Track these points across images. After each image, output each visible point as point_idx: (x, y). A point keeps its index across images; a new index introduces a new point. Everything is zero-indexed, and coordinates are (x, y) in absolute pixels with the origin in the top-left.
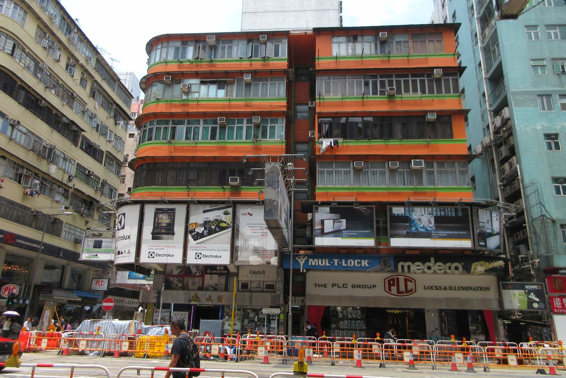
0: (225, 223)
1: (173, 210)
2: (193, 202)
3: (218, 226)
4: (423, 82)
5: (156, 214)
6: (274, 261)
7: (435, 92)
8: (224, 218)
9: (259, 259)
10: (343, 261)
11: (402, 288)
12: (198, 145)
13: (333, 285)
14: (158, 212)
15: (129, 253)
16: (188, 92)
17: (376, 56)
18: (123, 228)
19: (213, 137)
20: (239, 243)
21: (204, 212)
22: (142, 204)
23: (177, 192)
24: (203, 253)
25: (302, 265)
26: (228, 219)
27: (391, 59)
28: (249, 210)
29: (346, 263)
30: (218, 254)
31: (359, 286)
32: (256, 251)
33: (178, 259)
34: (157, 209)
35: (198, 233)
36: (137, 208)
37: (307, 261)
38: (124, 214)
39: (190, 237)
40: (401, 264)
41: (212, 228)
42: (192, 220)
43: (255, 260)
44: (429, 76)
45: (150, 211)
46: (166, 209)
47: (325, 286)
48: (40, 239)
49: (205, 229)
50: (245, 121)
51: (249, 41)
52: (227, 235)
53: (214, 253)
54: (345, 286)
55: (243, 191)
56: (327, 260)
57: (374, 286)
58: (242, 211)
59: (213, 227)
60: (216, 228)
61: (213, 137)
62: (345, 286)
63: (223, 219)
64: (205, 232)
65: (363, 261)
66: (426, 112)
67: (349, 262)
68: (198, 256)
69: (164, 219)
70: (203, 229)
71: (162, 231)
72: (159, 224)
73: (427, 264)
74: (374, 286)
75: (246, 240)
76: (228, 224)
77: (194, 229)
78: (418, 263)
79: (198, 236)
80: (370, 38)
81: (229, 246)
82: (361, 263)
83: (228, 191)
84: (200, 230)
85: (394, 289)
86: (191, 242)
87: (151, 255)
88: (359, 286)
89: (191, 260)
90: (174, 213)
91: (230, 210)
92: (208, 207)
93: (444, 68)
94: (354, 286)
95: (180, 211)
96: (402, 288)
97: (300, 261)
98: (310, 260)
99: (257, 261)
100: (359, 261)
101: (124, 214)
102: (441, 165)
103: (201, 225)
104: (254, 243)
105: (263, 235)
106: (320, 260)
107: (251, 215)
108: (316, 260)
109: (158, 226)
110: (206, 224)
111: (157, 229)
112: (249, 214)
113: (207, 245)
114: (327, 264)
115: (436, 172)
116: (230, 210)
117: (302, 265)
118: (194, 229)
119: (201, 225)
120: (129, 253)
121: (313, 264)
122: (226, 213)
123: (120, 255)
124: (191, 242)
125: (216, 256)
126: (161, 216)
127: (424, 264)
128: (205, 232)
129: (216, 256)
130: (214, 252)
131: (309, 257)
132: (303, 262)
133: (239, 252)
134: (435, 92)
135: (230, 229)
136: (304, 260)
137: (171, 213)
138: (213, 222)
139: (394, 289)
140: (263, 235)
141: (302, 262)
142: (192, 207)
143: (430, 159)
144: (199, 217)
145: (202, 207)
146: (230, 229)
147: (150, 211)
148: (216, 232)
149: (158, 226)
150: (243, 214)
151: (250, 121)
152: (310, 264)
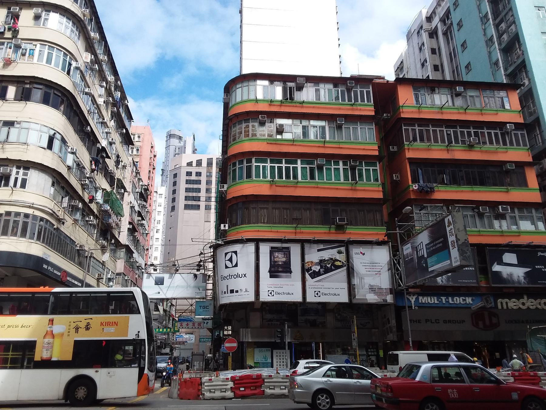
0: (340, 261)
1: (288, 248)
2: (309, 241)
3: (333, 265)
4: (496, 135)
5: (271, 253)
6: (390, 299)
7: (508, 144)
8: (338, 257)
9: (376, 297)
10: (450, 299)
11: (487, 322)
12: (299, 185)
13: (427, 321)
14: (273, 251)
15: (246, 291)
16: (280, 130)
17: (453, 107)
18: (236, 265)
19: (312, 177)
20: (356, 281)
21: (319, 250)
22: (257, 242)
23: (285, 231)
24: (275, 290)
25: (413, 302)
26: (342, 258)
27: (467, 111)
28: (361, 250)
29: (453, 300)
30: (337, 292)
31: (450, 321)
32: (372, 289)
33: (297, 298)
34: (272, 248)
35: (314, 271)
36: (251, 247)
37: (417, 299)
38: (236, 252)
39: (307, 276)
40: (499, 300)
41: (328, 267)
42: (307, 258)
43: (372, 298)
44: (501, 129)
45: (265, 249)
46: (280, 247)
47: (419, 321)
48: (81, 277)
49: (321, 267)
50: (341, 163)
51: (335, 86)
52: (342, 273)
53: (332, 291)
54: (437, 321)
55: (348, 231)
56: (436, 298)
57: (463, 321)
58: (355, 251)
59: (329, 266)
60: (331, 266)
61: (312, 177)
62: (437, 321)
63: (338, 258)
64: (322, 270)
65: (467, 298)
66: (505, 162)
67: (455, 299)
68: (317, 294)
69: (280, 258)
70: (319, 267)
71: (279, 270)
72: (275, 262)
73: (522, 301)
74: (463, 321)
75: (361, 279)
76: (343, 263)
77: (311, 267)
78: (514, 300)
79: (314, 275)
80: (446, 91)
81: (345, 285)
82: (465, 300)
83: (333, 230)
84: (317, 268)
85: (481, 324)
86: (310, 281)
87: (317, 294)
88: (450, 321)
89: (311, 298)
90: (290, 252)
91: (343, 249)
92: (322, 247)
93: (515, 124)
94: (445, 322)
95: (295, 250)
96: (487, 322)
97: (410, 299)
98: (420, 298)
99: (375, 299)
100: (464, 298)
101: (236, 252)
102: (520, 210)
103: (316, 264)
104: (369, 281)
105: (376, 274)
106: (429, 299)
107: (364, 254)
108: (425, 298)
109: (274, 265)
110: (321, 262)
111: (274, 267)
112: (361, 253)
113: (326, 284)
114: (436, 302)
115: (517, 218)
116: (343, 249)
117: (413, 302)
118: (311, 267)
119: (316, 264)
120: (246, 291)
121: (424, 302)
122: (340, 252)
123: (235, 294)
124: (310, 281)
125: (335, 294)
126: (276, 254)
127: (518, 300)
128: (322, 270)
129: (335, 294)
130: (331, 290)
131: (419, 294)
132: (414, 300)
133: (356, 290)
134: (508, 144)
135: (345, 268)
136: (414, 298)
137: (287, 252)
138: (328, 260)
139: (481, 324)
140: (376, 274)
141: (413, 299)
142: (307, 246)
143: (514, 205)
144: (314, 256)
145: (316, 247)
146: (345, 268)
147: (265, 249)
148: (332, 270)
149: (274, 265)
150: (357, 254)
151: (345, 164)
152: (420, 302)
